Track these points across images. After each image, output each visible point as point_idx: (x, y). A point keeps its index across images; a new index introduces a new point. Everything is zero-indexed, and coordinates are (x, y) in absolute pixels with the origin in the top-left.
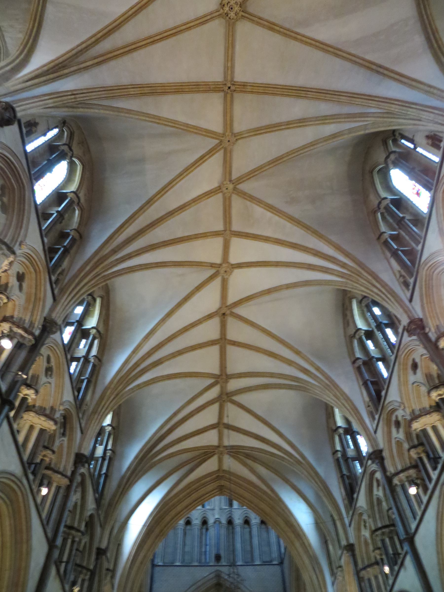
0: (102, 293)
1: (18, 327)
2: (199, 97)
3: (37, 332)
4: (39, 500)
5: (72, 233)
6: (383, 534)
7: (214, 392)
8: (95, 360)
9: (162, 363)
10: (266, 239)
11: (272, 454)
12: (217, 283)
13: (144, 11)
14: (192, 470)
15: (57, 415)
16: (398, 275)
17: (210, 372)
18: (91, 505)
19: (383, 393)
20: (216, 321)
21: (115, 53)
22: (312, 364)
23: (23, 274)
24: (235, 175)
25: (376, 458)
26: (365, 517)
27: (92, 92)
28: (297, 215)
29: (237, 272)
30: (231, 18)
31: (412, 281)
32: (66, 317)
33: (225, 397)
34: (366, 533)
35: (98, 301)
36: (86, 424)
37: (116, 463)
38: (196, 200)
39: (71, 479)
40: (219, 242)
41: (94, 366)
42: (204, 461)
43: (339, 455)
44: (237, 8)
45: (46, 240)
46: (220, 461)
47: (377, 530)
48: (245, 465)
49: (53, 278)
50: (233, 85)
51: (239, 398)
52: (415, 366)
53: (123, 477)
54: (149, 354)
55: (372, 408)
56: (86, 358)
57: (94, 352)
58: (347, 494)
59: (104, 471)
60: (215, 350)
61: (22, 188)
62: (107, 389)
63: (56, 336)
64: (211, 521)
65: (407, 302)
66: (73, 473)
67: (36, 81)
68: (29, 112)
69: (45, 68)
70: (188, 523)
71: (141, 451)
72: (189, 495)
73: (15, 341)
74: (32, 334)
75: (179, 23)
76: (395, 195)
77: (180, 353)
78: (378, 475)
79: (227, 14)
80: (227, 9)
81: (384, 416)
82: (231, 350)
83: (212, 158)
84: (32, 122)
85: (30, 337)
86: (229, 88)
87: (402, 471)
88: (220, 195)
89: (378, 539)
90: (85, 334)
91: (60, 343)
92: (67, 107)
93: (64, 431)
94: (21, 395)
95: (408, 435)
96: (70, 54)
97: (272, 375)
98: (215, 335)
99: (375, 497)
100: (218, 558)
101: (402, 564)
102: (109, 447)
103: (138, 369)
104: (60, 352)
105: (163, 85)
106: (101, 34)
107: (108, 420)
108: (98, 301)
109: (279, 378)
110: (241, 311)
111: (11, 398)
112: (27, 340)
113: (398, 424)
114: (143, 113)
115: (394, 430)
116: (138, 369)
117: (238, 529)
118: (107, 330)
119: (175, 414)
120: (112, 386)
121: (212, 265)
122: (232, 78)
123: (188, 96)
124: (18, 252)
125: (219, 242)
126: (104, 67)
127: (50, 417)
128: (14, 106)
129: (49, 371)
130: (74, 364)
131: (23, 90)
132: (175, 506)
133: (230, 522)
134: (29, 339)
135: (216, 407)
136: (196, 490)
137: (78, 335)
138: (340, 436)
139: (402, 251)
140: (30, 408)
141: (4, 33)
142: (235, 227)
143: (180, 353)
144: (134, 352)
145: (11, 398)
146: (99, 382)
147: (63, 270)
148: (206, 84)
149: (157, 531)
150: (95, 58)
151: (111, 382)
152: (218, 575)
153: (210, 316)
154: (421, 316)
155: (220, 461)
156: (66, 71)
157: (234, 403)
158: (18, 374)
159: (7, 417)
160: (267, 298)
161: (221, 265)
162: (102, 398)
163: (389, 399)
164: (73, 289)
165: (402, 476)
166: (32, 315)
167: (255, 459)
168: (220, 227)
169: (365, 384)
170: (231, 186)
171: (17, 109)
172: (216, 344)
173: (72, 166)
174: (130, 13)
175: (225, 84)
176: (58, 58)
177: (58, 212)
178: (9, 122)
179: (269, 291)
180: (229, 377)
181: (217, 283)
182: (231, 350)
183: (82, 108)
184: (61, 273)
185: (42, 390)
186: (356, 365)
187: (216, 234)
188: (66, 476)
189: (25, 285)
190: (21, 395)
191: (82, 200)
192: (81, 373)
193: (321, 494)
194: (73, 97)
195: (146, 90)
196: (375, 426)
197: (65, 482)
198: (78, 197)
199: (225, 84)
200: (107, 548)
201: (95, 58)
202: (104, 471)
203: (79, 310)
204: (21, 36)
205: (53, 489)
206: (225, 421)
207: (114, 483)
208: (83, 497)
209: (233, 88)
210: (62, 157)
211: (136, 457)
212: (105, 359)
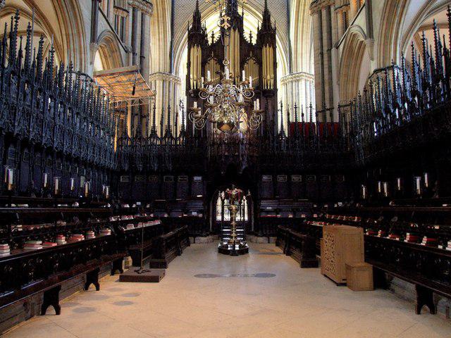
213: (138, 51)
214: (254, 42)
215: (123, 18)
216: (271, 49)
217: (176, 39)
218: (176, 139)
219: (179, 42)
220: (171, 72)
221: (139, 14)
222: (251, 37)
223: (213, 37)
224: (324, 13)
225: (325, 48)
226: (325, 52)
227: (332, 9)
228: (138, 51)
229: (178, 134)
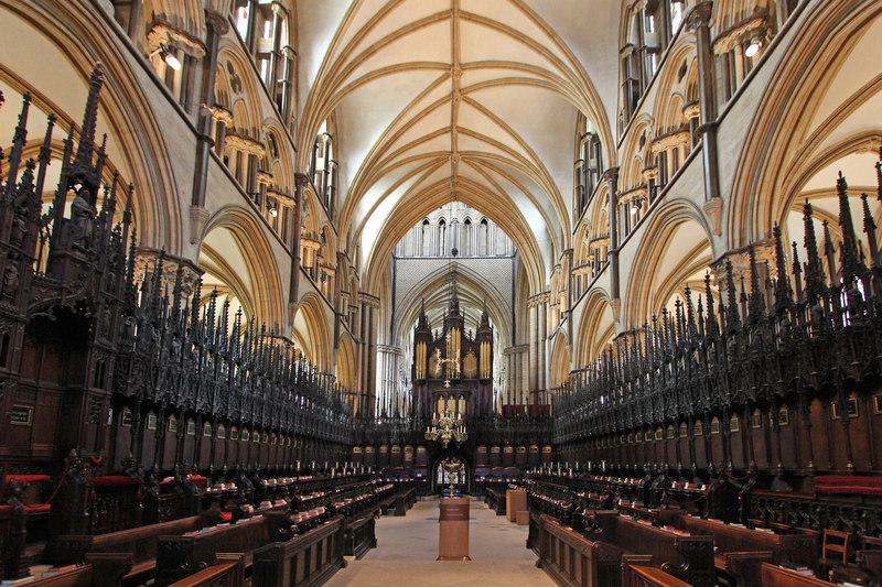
1: (177, 32)
3: (203, 37)
4: (271, 223)
7: (445, 88)
8: (288, 53)
9: (375, 52)
11: (510, 162)
14: (428, 174)
15: (263, 138)
17: (440, 61)
19: (639, 102)
22: (567, 53)
25: (610, 176)
36: (298, 140)
41: (290, 61)
42: (437, 167)
43: (581, 164)
46: (454, 167)
48: (481, 171)
51: (474, 96)
52: (683, 71)
54: (356, 41)
55: (623, 118)
56: (278, 54)
57: (284, 41)
58: (579, 206)
59: (329, 183)
60: (446, 25)
64: (448, 222)
70: (426, 222)
71: (366, 161)
72: (423, 201)
73: (181, 54)
74: (199, 42)
85: (197, 46)
87: (631, 191)
93: (276, 151)
94: (215, 120)
97: (516, 66)
102: (330, 158)
104: (241, 54)
107: (323, 129)
109: (526, 70)
112: (195, 51)
117: (474, 228)
119: (399, 118)
127: (255, 141)
129: (235, 83)
132: (408, 212)
135: (448, 106)
138: (586, 144)
140: (231, 132)
144: (336, 39)
146: (301, 85)
151: (315, 85)
155: (454, 167)
157: (470, 102)
159: (211, 153)
162: (308, 108)
163: (642, 111)
165: (629, 196)
166: (187, 9)
167: (491, 166)
172: (445, 19)
180: (464, 67)
185: (235, 110)
186: (623, 55)
190: (215, 120)
193: (553, 203)
200: (347, 252)
202: (329, 183)
205: (281, 209)
206: (460, 123)
207: (343, 195)
212: (301, 50)
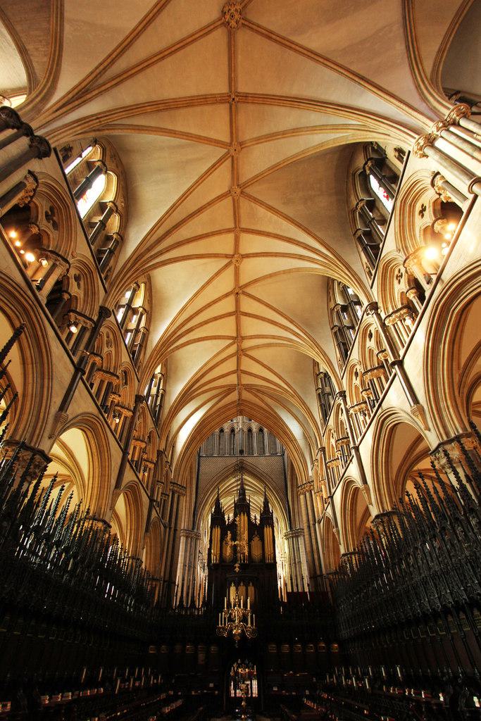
0: (145, 280)
2: (207, 109)
5: (115, 236)
6: (343, 442)
7: (233, 349)
10: (268, 235)
12: (231, 270)
13: (153, 24)
16: (365, 267)
18: (150, 425)
19: (349, 353)
20: (231, 299)
21: (130, 73)
23: (79, 275)
24: (243, 180)
26: (332, 431)
27: (114, 114)
28: (291, 215)
29: (245, 260)
30: (233, 26)
31: (373, 272)
32: (117, 303)
33: (240, 352)
34: (333, 441)
35: (143, 286)
37: (167, 398)
38: (210, 204)
39: (134, 412)
40: (230, 237)
41: (144, 334)
43: (320, 391)
44: (237, 16)
45: (93, 247)
47: (339, 440)
49: (103, 276)
50: (237, 96)
51: (250, 353)
53: (172, 406)
54: (183, 325)
56: (137, 330)
57: (143, 324)
59: (158, 403)
60: (233, 319)
61: (66, 207)
62: (154, 350)
63: (112, 318)
65: (369, 288)
66: (135, 408)
67: (64, 110)
68: (62, 141)
69: (70, 96)
70: (222, 431)
71: (183, 389)
72: (219, 416)
75: (185, 35)
76: (371, 196)
77: (206, 322)
78: (342, 406)
79: (228, 23)
80: (228, 17)
81: (348, 368)
82: (244, 319)
83: (222, 166)
84: (68, 147)
86: (233, 99)
88: (230, 198)
89: (339, 446)
90: (135, 311)
91: (115, 323)
92: (94, 131)
95: (363, 383)
96: (91, 78)
97: (274, 337)
98: (232, 309)
99: (339, 420)
100: (242, 452)
101: (351, 461)
102: (161, 387)
103: (176, 336)
105: (175, 100)
106: (115, 54)
107: (158, 370)
108: (143, 286)
110: (249, 290)
111: (82, 367)
113: (357, 374)
114: (161, 129)
115: (354, 377)
116: (176, 336)
117: (255, 435)
118: (151, 308)
119: (205, 365)
120: (158, 348)
121: (226, 256)
122: (236, 88)
123: (198, 109)
124: (71, 261)
125: (230, 237)
126: (122, 87)
128: (47, 138)
130: (129, 334)
131: (54, 120)
132: (210, 422)
133: (250, 430)
134: (89, 325)
136: (224, 412)
137: (130, 312)
139: (370, 246)
141: (32, 58)
142: (243, 225)
143: (206, 322)
145: (82, 367)
147: (110, 268)
148: (213, 96)
149: (198, 438)
150: (113, 79)
151: (157, 346)
152: (242, 462)
153: (227, 295)
154: (377, 301)
155: (240, 394)
156: (89, 96)
158: (83, 352)
160: (269, 280)
161: (233, 255)
164: (121, 280)
167: (263, 393)
168: (231, 225)
169: (339, 345)
170: (239, 191)
171: (50, 142)
173: (109, 182)
174: (140, 28)
175: (230, 96)
176: (80, 84)
177: (100, 221)
178: (47, 154)
179: (271, 276)
180: (243, 338)
181: (231, 270)
182: (244, 319)
183: (107, 129)
184: (109, 270)
187: (229, 231)
188: (130, 410)
189: (82, 283)
191: (120, 208)
192: (134, 340)
194: (98, 121)
195: (161, 107)
196: (342, 375)
197: (131, 414)
198: (116, 206)
199: (230, 96)
201: (113, 79)
203: (128, 294)
204: (45, 59)
206: (243, 368)
208: (145, 421)
209: (237, 99)
210: (99, 171)
211: (180, 394)
213: (173, 525)
214: (258, 522)
215: (165, 500)
216: (271, 529)
217: (199, 500)
218: (198, 609)
219: (200, 504)
220: (193, 529)
221: (176, 495)
222: (255, 519)
223: (229, 519)
224: (308, 494)
225: (311, 522)
226: (311, 525)
227: (313, 492)
228: (173, 525)
229: (201, 603)
